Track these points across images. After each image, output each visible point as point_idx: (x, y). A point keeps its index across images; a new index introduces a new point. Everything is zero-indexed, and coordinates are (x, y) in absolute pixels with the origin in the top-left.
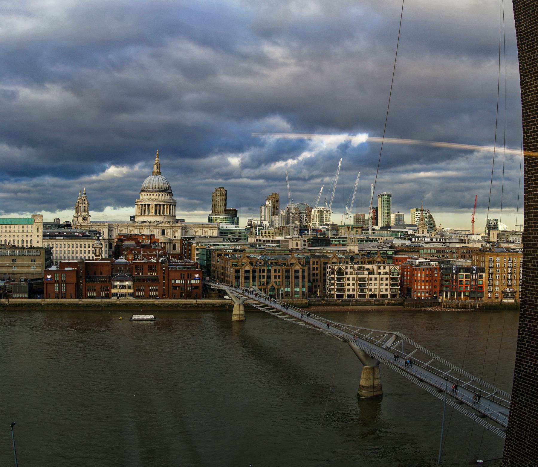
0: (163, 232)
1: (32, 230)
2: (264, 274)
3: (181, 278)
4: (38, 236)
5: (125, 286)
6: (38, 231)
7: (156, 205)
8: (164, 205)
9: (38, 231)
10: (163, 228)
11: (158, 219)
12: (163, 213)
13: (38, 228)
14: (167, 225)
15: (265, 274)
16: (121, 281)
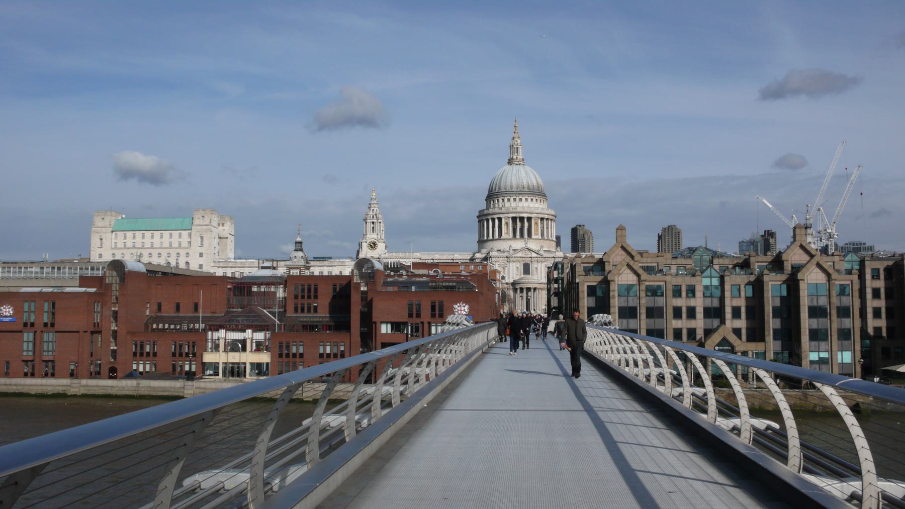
0: (527, 269)
1: (190, 243)
2: (692, 303)
3: (411, 315)
4: (201, 255)
5: (244, 342)
6: (202, 245)
7: (514, 219)
8: (529, 219)
9: (202, 245)
10: (528, 260)
11: (518, 244)
12: (530, 235)
13: (202, 238)
14: (534, 255)
15: (699, 303)
16: (228, 329)
